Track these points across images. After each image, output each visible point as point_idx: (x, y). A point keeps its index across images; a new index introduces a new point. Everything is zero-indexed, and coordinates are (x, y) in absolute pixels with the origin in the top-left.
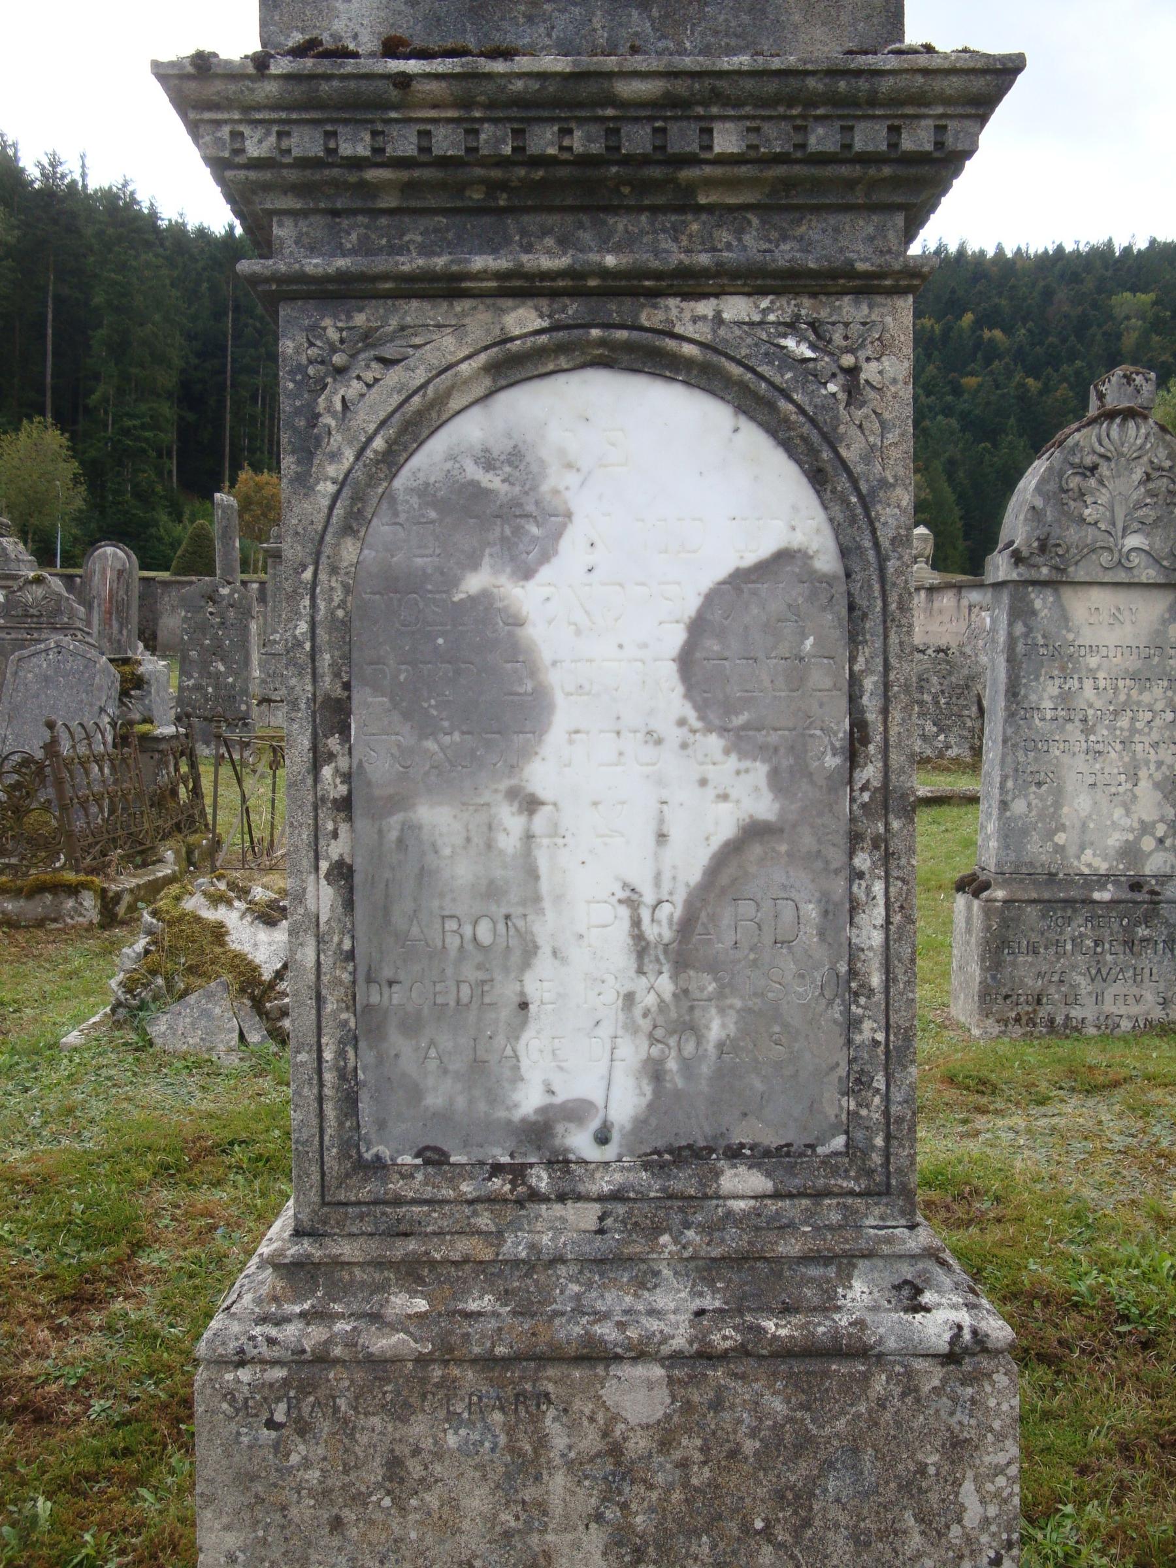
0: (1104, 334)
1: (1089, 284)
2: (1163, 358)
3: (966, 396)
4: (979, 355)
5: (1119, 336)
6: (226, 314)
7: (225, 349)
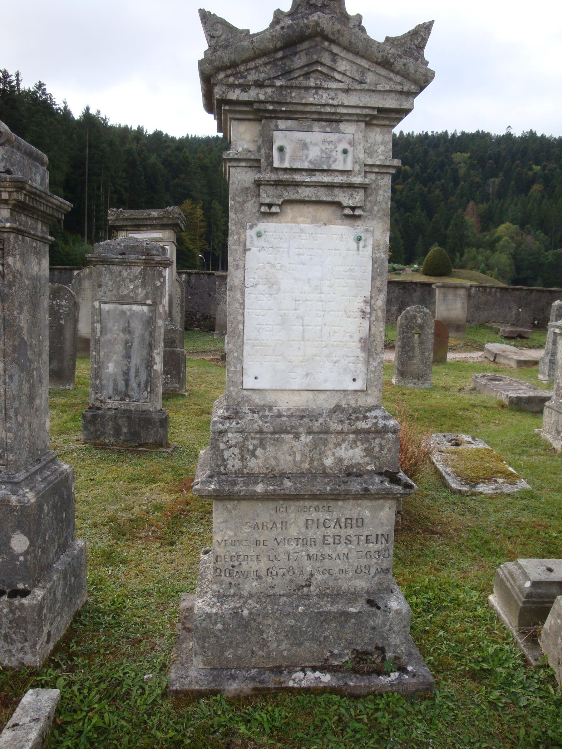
0: (451, 169)
1: (442, 149)
2: (477, 180)
3: (398, 193)
4: (401, 176)
5: (457, 170)
6: (85, 149)
7: (84, 165)
